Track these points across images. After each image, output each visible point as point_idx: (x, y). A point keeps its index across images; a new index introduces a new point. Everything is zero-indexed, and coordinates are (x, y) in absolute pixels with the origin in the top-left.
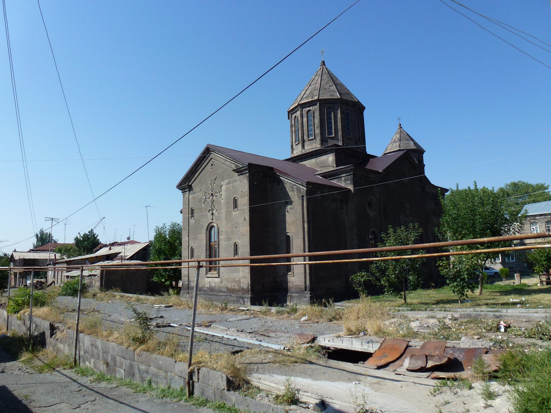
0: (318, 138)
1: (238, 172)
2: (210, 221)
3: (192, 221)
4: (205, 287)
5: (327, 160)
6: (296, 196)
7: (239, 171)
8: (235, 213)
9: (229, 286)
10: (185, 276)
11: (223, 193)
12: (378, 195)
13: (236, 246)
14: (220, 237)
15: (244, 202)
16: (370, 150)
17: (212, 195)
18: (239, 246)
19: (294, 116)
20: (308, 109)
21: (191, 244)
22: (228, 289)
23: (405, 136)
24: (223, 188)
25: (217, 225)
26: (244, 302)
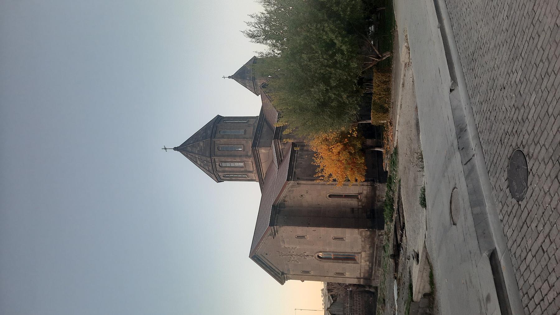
0: (244, 159)
1: (275, 234)
3: (312, 273)
4: (369, 265)
6: (298, 188)
7: (274, 234)
8: (308, 237)
9: (368, 246)
10: (359, 281)
11: (291, 246)
13: (336, 238)
14: (328, 250)
16: (256, 113)
19: (222, 178)
20: (218, 166)
21: (332, 274)
22: (370, 247)
24: (287, 246)
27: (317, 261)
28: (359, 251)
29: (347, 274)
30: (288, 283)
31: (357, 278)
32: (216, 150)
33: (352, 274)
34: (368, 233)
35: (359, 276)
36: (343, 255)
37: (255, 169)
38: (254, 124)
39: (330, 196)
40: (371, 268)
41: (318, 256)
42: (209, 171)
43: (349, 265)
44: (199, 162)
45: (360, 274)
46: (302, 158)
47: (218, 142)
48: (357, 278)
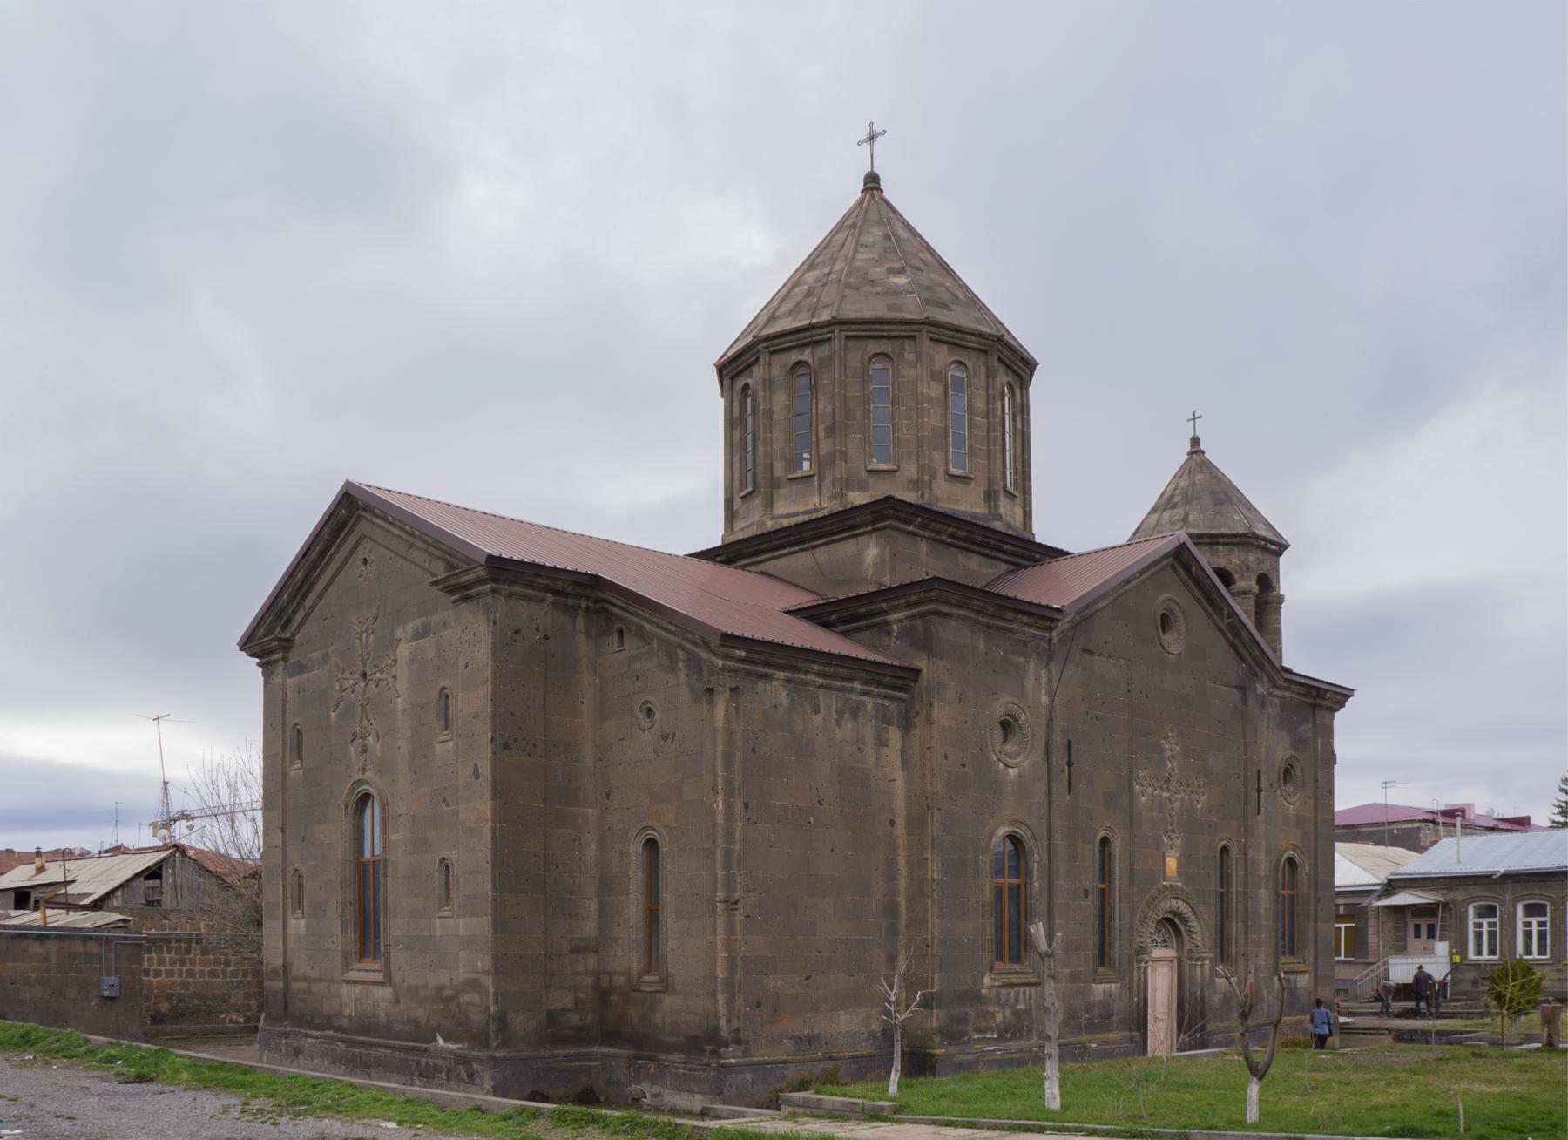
2: (356, 778)
5: (858, 558)
8: (445, 747)
12: (1045, 699)
15: (474, 702)
17: (364, 674)
18: (454, 872)
19: (739, 385)
20: (794, 357)
23: (1201, 481)
25: (380, 792)
26: (471, 1076)
27: (344, 793)
28: (397, 976)
29: (298, 925)
30: (251, 668)
31: (286, 967)
32: (872, 347)
33: (300, 940)
34: (477, 1018)
35: (295, 971)
36: (376, 913)
37: (786, 523)
38: (999, 517)
39: (651, 844)
40: (326, 1023)
41: (366, 797)
42: (772, 319)
43: (338, 934)
44: (810, 277)
45: (306, 979)
46: (840, 712)
47: (910, 356)
48: (286, 967)
